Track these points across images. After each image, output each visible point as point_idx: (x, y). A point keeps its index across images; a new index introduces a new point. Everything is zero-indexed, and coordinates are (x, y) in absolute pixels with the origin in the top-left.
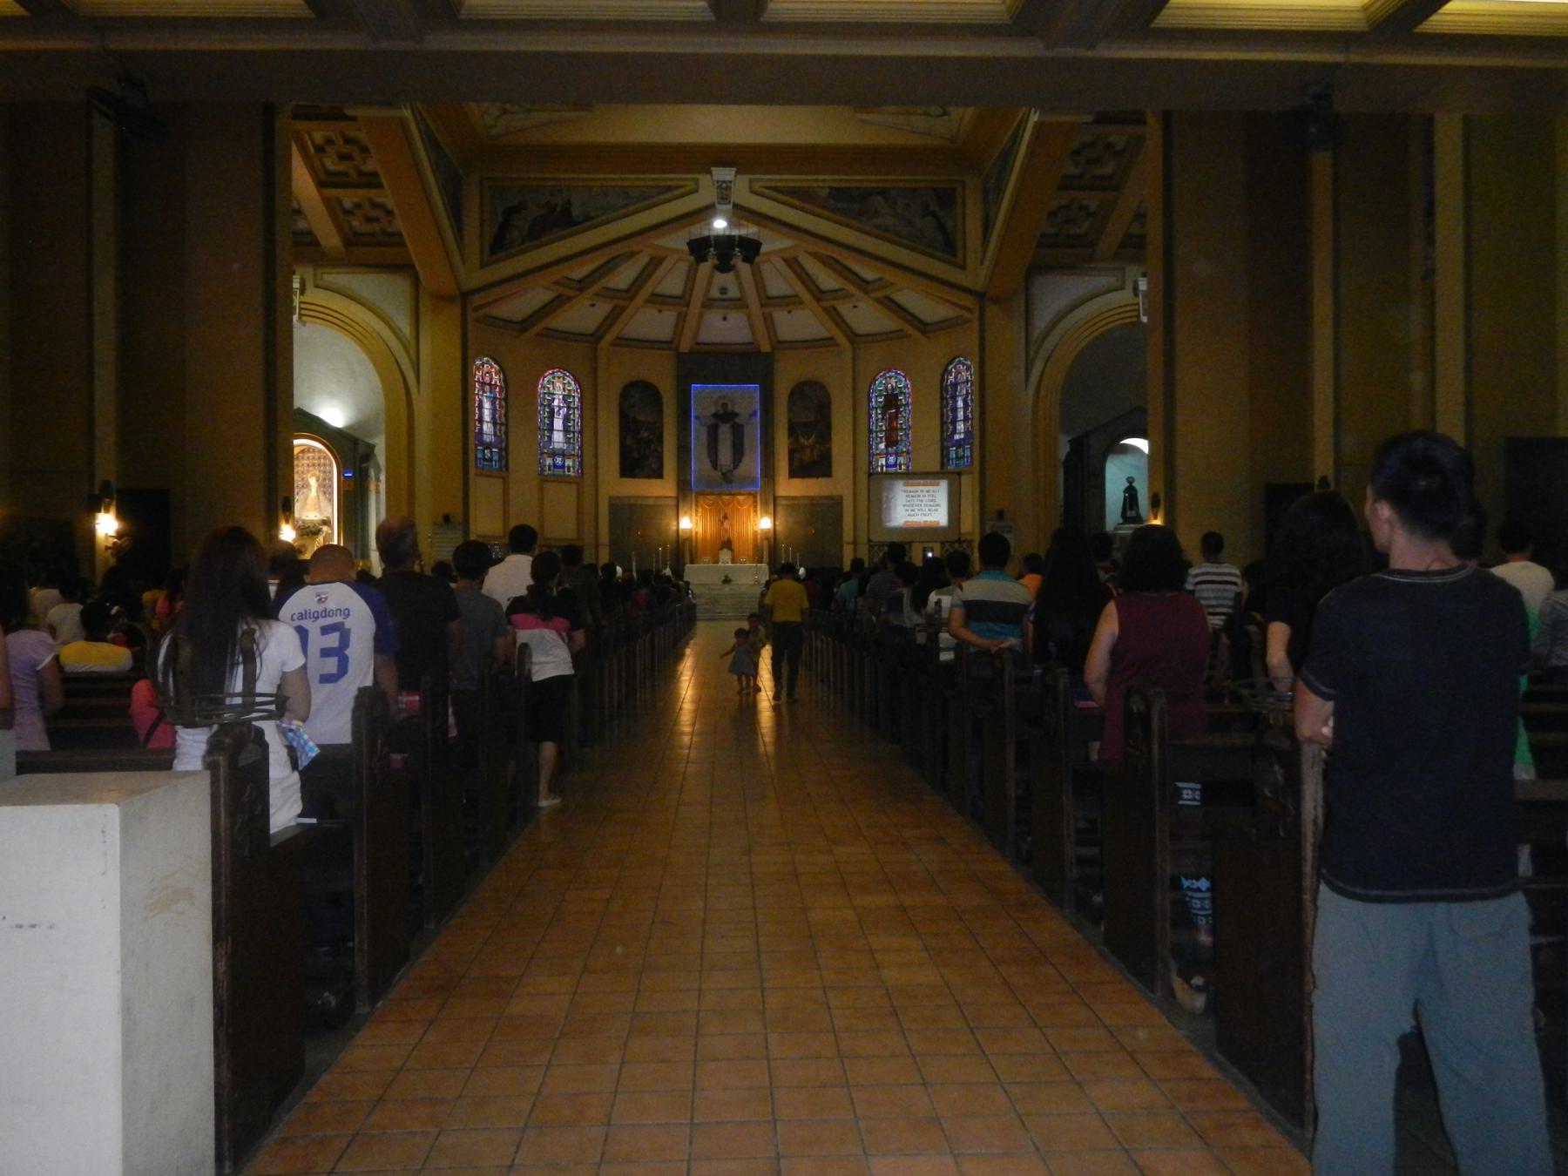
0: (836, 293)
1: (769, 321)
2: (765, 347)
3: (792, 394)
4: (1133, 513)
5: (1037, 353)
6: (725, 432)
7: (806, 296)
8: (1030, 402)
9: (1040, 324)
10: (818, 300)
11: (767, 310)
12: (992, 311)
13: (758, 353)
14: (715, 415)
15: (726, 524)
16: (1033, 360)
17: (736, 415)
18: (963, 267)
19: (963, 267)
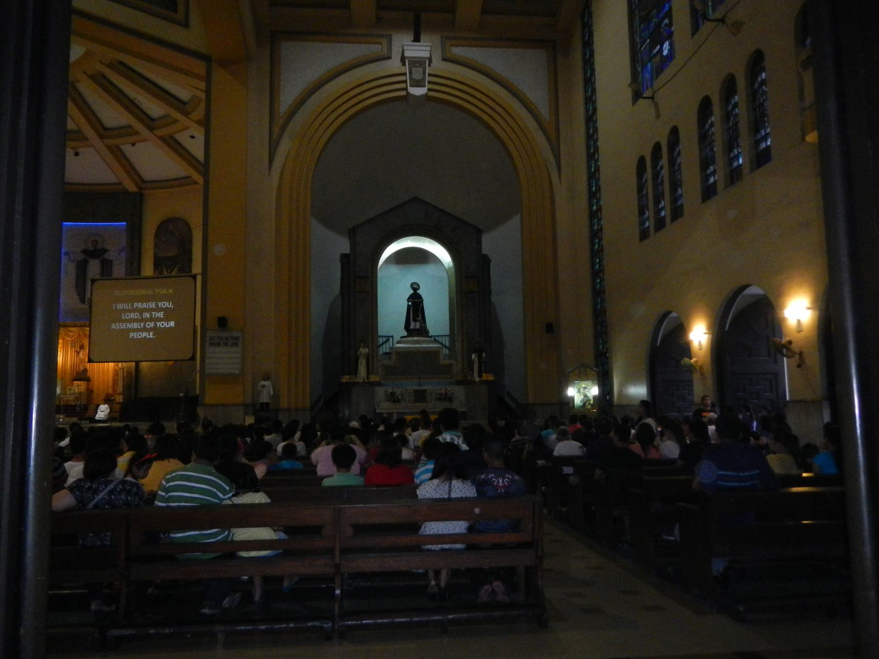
0: (166, 121)
1: (118, 154)
2: (131, 187)
3: (159, 228)
4: (418, 326)
5: (283, 128)
6: (94, 268)
7: (138, 126)
8: (275, 185)
9: (288, 97)
10: (151, 129)
11: (110, 142)
12: (219, 75)
13: (126, 193)
14: (85, 252)
15: (81, 354)
16: (278, 142)
17: (105, 251)
18: (186, 25)
19: (186, 25)
